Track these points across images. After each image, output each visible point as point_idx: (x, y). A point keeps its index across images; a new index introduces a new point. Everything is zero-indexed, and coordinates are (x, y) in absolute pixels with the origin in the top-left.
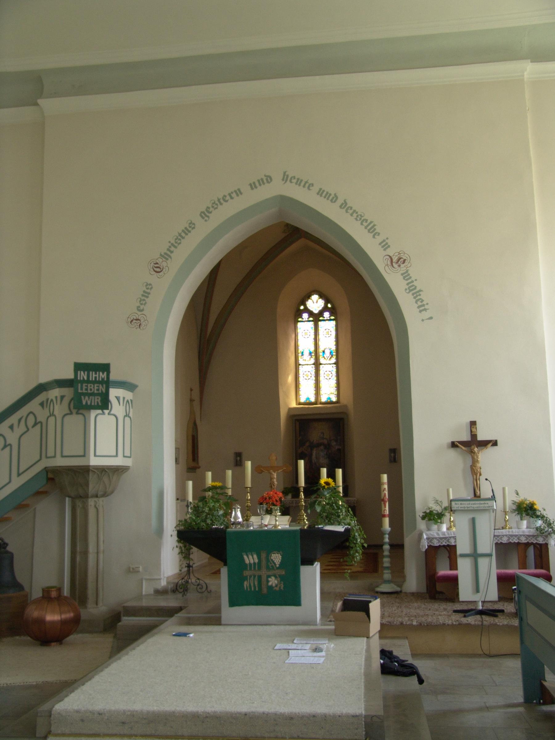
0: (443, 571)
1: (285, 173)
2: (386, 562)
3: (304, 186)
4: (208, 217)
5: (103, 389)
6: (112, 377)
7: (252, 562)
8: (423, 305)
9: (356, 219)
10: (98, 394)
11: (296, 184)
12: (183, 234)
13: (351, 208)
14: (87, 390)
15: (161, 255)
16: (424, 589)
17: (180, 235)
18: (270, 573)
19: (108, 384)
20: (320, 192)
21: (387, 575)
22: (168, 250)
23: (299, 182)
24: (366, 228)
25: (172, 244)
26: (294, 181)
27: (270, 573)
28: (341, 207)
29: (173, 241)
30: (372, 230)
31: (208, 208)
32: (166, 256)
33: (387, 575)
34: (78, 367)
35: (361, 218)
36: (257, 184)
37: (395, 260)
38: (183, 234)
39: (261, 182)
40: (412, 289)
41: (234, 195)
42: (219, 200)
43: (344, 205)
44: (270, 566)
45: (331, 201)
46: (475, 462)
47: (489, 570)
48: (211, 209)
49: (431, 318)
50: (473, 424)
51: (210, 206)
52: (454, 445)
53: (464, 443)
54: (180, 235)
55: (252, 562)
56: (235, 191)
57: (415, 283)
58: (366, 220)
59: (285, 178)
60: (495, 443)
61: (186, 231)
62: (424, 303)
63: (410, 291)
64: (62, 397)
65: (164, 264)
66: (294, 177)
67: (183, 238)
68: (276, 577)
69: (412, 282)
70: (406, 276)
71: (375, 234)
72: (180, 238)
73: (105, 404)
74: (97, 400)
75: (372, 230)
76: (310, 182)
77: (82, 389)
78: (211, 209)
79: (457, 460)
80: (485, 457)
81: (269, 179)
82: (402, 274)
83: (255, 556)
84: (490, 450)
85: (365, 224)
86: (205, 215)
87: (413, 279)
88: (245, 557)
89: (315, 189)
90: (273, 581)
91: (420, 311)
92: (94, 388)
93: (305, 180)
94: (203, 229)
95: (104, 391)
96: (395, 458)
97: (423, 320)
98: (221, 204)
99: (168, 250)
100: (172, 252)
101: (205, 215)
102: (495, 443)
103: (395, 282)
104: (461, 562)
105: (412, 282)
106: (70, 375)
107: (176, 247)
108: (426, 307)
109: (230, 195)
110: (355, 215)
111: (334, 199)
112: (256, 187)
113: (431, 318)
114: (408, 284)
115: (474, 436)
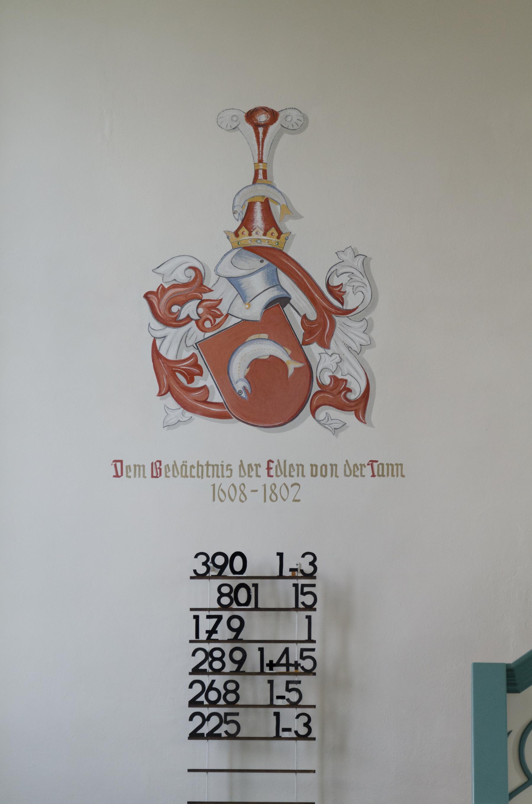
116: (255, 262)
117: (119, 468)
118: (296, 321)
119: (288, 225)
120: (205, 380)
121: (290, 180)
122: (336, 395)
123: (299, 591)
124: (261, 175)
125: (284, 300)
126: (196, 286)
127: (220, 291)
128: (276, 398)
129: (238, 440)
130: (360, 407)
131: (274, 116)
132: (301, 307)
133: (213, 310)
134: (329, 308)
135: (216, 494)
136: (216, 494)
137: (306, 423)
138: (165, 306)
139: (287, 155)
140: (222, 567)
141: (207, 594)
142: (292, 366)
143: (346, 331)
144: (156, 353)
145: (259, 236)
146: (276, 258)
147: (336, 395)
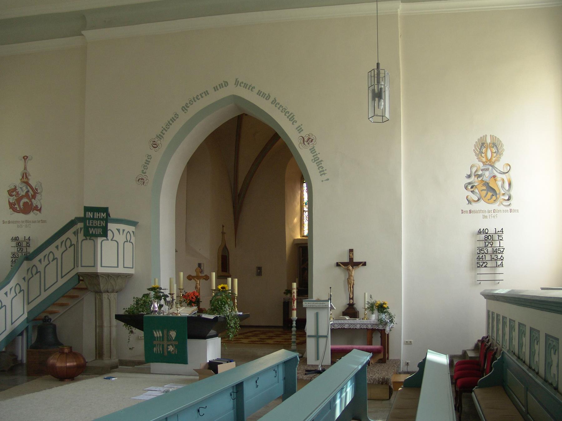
1: (237, 79)
3: (249, 89)
4: (187, 110)
7: (158, 336)
8: (323, 171)
9: (282, 112)
10: (100, 227)
11: (244, 87)
12: (171, 122)
13: (279, 104)
14: (92, 224)
15: (157, 136)
17: (169, 122)
18: (169, 343)
20: (259, 93)
22: (161, 132)
23: (245, 86)
24: (288, 117)
25: (164, 129)
26: (242, 85)
27: (169, 343)
28: (272, 103)
29: (164, 127)
30: (292, 118)
31: (187, 104)
32: (160, 137)
35: (285, 111)
36: (219, 88)
37: (306, 140)
38: (171, 122)
39: (221, 86)
41: (204, 95)
42: (194, 99)
43: (274, 102)
44: (169, 339)
45: (266, 99)
48: (189, 105)
49: (328, 180)
50: (351, 251)
51: (188, 102)
53: (345, 264)
54: (169, 122)
55: (158, 336)
56: (205, 92)
57: (318, 156)
58: (289, 112)
59: (237, 83)
61: (173, 120)
62: (324, 169)
63: (315, 161)
65: (159, 142)
66: (243, 82)
67: (171, 124)
68: (173, 346)
69: (317, 155)
70: (313, 150)
71: (294, 122)
72: (169, 124)
75: (292, 118)
76: (253, 86)
77: (89, 224)
78: (189, 105)
81: (226, 84)
82: (310, 150)
83: (160, 332)
85: (287, 115)
86: (185, 109)
87: (317, 153)
88: (155, 332)
89: (256, 91)
90: (171, 348)
91: (321, 175)
93: (249, 84)
94: (184, 118)
95: (104, 225)
97: (322, 181)
98: (195, 101)
99: (161, 132)
100: (164, 134)
101: (185, 109)
105: (317, 155)
107: (166, 131)
108: (325, 172)
109: (201, 95)
110: (281, 108)
111: (268, 98)
112: (218, 90)
113: (328, 180)
114: (313, 156)
115: (351, 259)
116: (24, 184)
117: (4, 222)
118: (30, 195)
119: (29, 177)
123: (27, 243)
124: (25, 168)
125: (28, 191)
126: (15, 189)
127: (19, 190)
128: (28, 209)
129: (21, 217)
131: (27, 157)
132: (31, 193)
133: (18, 193)
134: (35, 193)
135: (18, 226)
136: (18, 226)
137: (32, 213)
140: (16, 239)
141: (14, 244)
142: (30, 203)
143: (38, 196)
144: (9, 202)
145: (25, 180)
146: (27, 184)
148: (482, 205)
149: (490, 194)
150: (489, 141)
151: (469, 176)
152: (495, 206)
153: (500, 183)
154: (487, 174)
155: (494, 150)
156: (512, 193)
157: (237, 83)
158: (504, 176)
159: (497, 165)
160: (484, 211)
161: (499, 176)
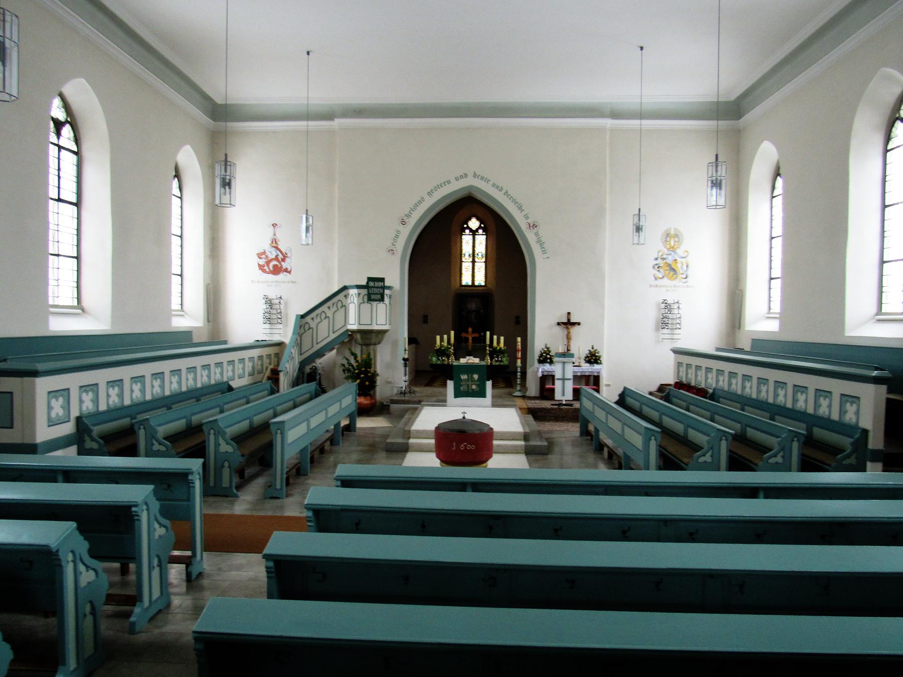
0: (548, 386)
2: (519, 381)
5: (381, 291)
6: (387, 284)
16: (538, 395)
19: (384, 288)
20: (494, 185)
21: (518, 388)
23: (482, 178)
30: (520, 208)
32: (408, 216)
33: (518, 388)
34: (370, 279)
39: (461, 177)
40: (540, 242)
43: (506, 193)
46: (569, 333)
47: (570, 386)
50: (569, 313)
52: (559, 324)
53: (563, 323)
59: (475, 175)
60: (579, 324)
61: (420, 202)
64: (359, 294)
70: (537, 234)
72: (416, 206)
73: (382, 299)
74: (379, 297)
75: (520, 208)
79: (560, 332)
80: (574, 330)
81: (466, 175)
84: (577, 327)
86: (430, 194)
89: (491, 183)
92: (376, 290)
96: (519, 324)
102: (579, 324)
103: (530, 236)
104: (557, 382)
106: (364, 283)
111: (501, 190)
115: (569, 320)
117: (253, 282)
120: (266, 268)
121: (278, 237)
122: (286, 270)
124: (275, 235)
126: (264, 253)
127: (268, 254)
128: (277, 270)
130: (289, 272)
132: (280, 256)
133: (267, 257)
138: (259, 256)
139: (278, 230)
143: (287, 260)
146: (277, 248)
147: (286, 270)
148: (666, 281)
149: (672, 273)
150: (672, 232)
151: (656, 259)
152: (675, 282)
153: (679, 265)
154: (670, 258)
155: (676, 239)
156: (689, 273)
157: (475, 175)
158: (683, 260)
159: (678, 251)
160: (666, 286)
161: (679, 260)
